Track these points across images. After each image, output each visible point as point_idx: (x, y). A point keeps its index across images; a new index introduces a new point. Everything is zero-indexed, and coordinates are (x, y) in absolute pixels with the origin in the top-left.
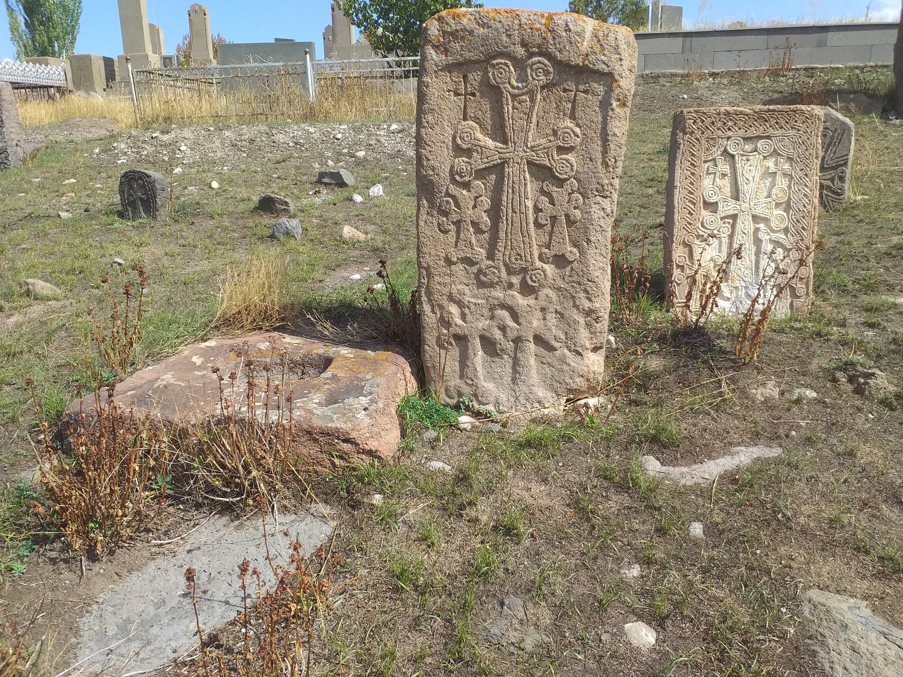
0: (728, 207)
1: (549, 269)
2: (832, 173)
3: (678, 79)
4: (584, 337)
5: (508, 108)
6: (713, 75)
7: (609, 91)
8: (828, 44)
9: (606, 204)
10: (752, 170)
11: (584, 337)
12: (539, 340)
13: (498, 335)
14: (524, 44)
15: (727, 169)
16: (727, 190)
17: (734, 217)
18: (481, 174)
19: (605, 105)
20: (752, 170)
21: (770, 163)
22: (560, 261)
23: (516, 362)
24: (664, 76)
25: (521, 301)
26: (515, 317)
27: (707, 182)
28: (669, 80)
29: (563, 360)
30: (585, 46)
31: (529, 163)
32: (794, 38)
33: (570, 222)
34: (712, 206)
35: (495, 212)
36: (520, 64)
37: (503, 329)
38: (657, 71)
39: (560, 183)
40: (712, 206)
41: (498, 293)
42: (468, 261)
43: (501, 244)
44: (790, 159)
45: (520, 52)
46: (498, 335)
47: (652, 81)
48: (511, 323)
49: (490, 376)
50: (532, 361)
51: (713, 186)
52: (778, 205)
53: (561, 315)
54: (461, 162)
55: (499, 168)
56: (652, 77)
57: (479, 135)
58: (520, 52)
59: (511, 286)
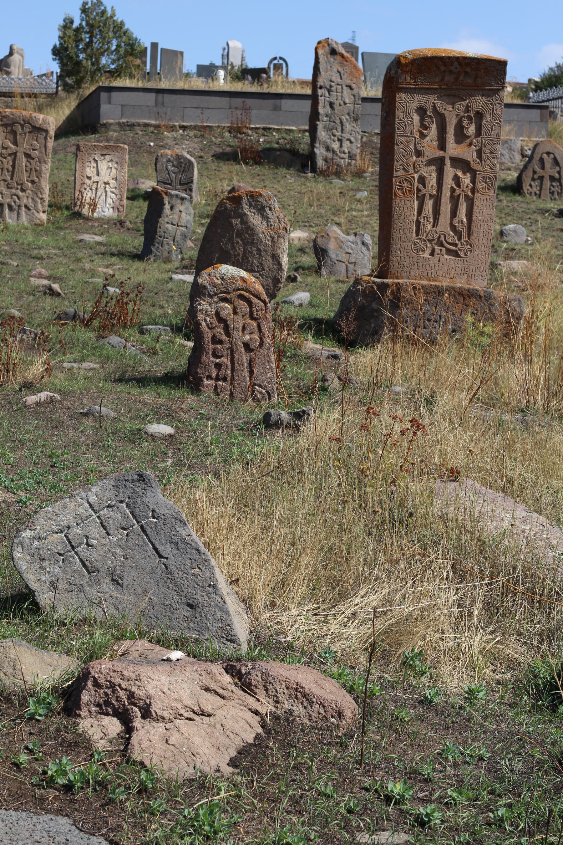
0: (95, 178)
1: (29, 184)
2: (186, 187)
3: (152, 129)
4: (40, 206)
5: (18, 137)
6: (184, 128)
7: (47, 135)
8: (283, 108)
9: (46, 166)
10: (103, 166)
11: (40, 206)
12: (26, 207)
13: (13, 204)
14: (23, 120)
15: (95, 165)
16: (95, 172)
17: (97, 182)
18: (10, 155)
19: (46, 138)
20: (103, 166)
21: (110, 164)
22: (33, 182)
23: (18, 214)
24: (139, 125)
25: (20, 194)
26: (19, 198)
27: (88, 169)
28: (142, 128)
29: (33, 214)
30: (40, 122)
31: (24, 153)
32: (250, 102)
33: (36, 171)
34: (89, 178)
35: (13, 166)
36: (22, 126)
37: (15, 202)
38: (133, 120)
39: (33, 159)
40: (89, 178)
41: (14, 191)
42: (5, 180)
43: (15, 176)
44: (117, 163)
45: (22, 122)
46: (13, 204)
47: (128, 128)
48: (17, 200)
49: (10, 218)
50: (24, 213)
51: (90, 171)
52: (113, 179)
53: (33, 199)
54: (4, 151)
55: (15, 154)
56: (128, 126)
57: (10, 144)
58: (22, 122)
59: (17, 189)
